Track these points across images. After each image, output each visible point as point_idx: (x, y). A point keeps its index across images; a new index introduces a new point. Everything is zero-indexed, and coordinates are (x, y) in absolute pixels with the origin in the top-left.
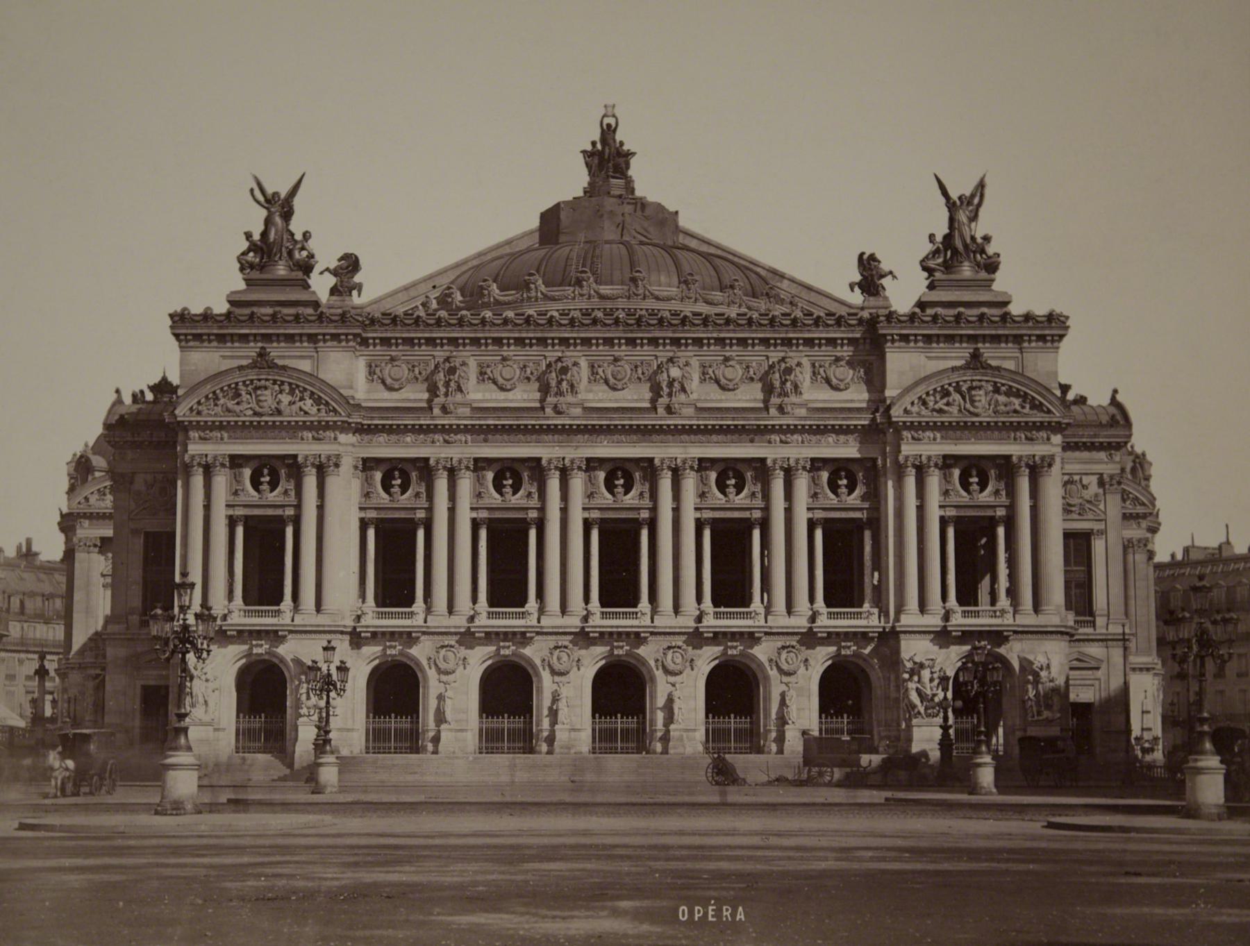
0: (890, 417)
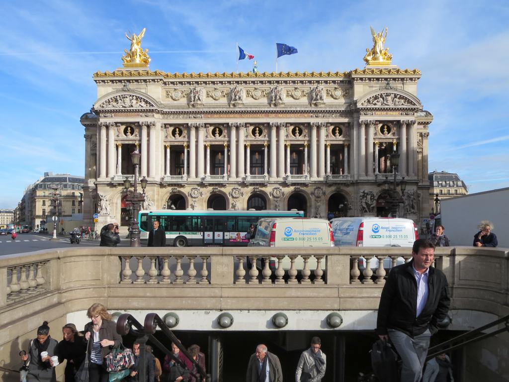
0: (356, 106)
